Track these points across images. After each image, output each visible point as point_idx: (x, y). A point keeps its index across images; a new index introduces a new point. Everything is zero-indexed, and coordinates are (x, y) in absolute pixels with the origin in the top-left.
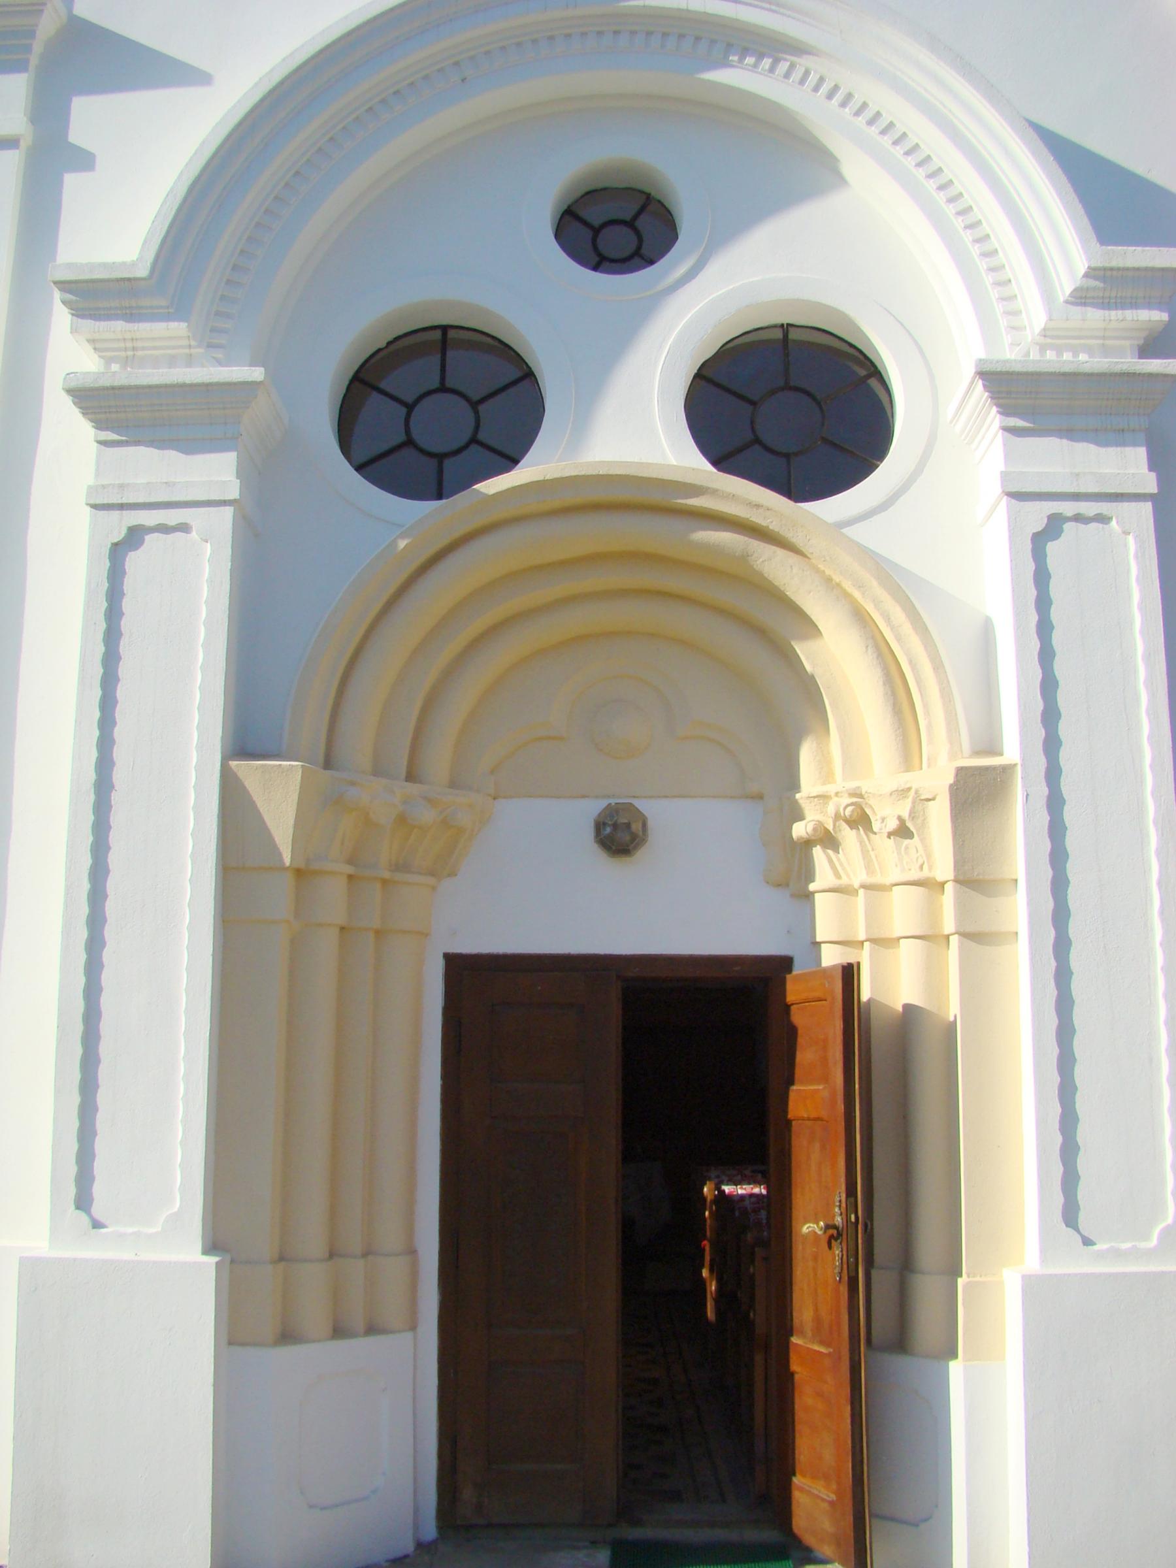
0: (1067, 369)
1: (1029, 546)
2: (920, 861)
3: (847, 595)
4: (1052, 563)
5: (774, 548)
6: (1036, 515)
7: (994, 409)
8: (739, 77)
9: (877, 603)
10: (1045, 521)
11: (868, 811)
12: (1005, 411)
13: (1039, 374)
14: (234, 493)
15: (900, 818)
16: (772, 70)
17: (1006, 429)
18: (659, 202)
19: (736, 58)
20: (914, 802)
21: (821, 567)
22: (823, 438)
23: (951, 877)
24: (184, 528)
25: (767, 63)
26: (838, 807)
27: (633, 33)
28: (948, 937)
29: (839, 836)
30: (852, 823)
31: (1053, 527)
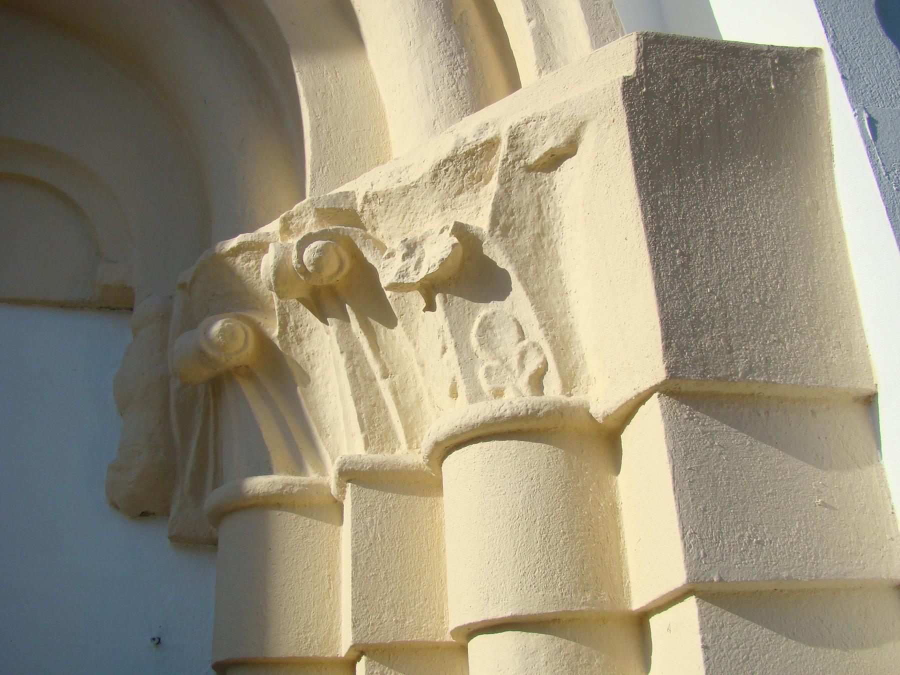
2: (533, 363)
11: (370, 256)
15: (460, 230)
20: (506, 180)
23: (655, 371)
26: (286, 250)
28: (641, 620)
29: (298, 354)
30: (324, 301)
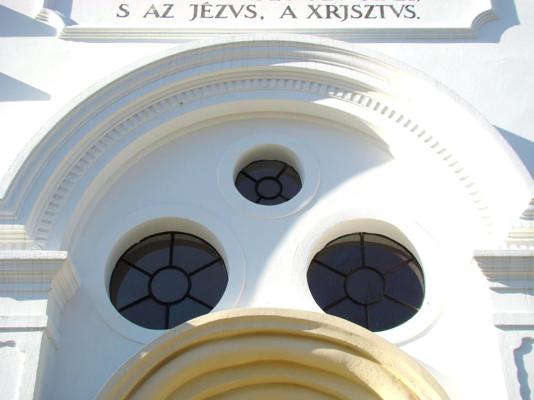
0: (526, 254)
1: (512, 356)
3: (404, 386)
4: (527, 366)
5: (361, 358)
6: (515, 339)
7: (485, 278)
8: (334, 103)
9: (423, 391)
10: (521, 342)
12: (492, 279)
13: (510, 257)
14: (44, 323)
16: (351, 99)
17: (493, 289)
18: (292, 167)
19: (332, 93)
21: (389, 369)
22: (385, 296)
24: (11, 344)
25: (349, 95)
27: (278, 80)
31: (526, 346)
